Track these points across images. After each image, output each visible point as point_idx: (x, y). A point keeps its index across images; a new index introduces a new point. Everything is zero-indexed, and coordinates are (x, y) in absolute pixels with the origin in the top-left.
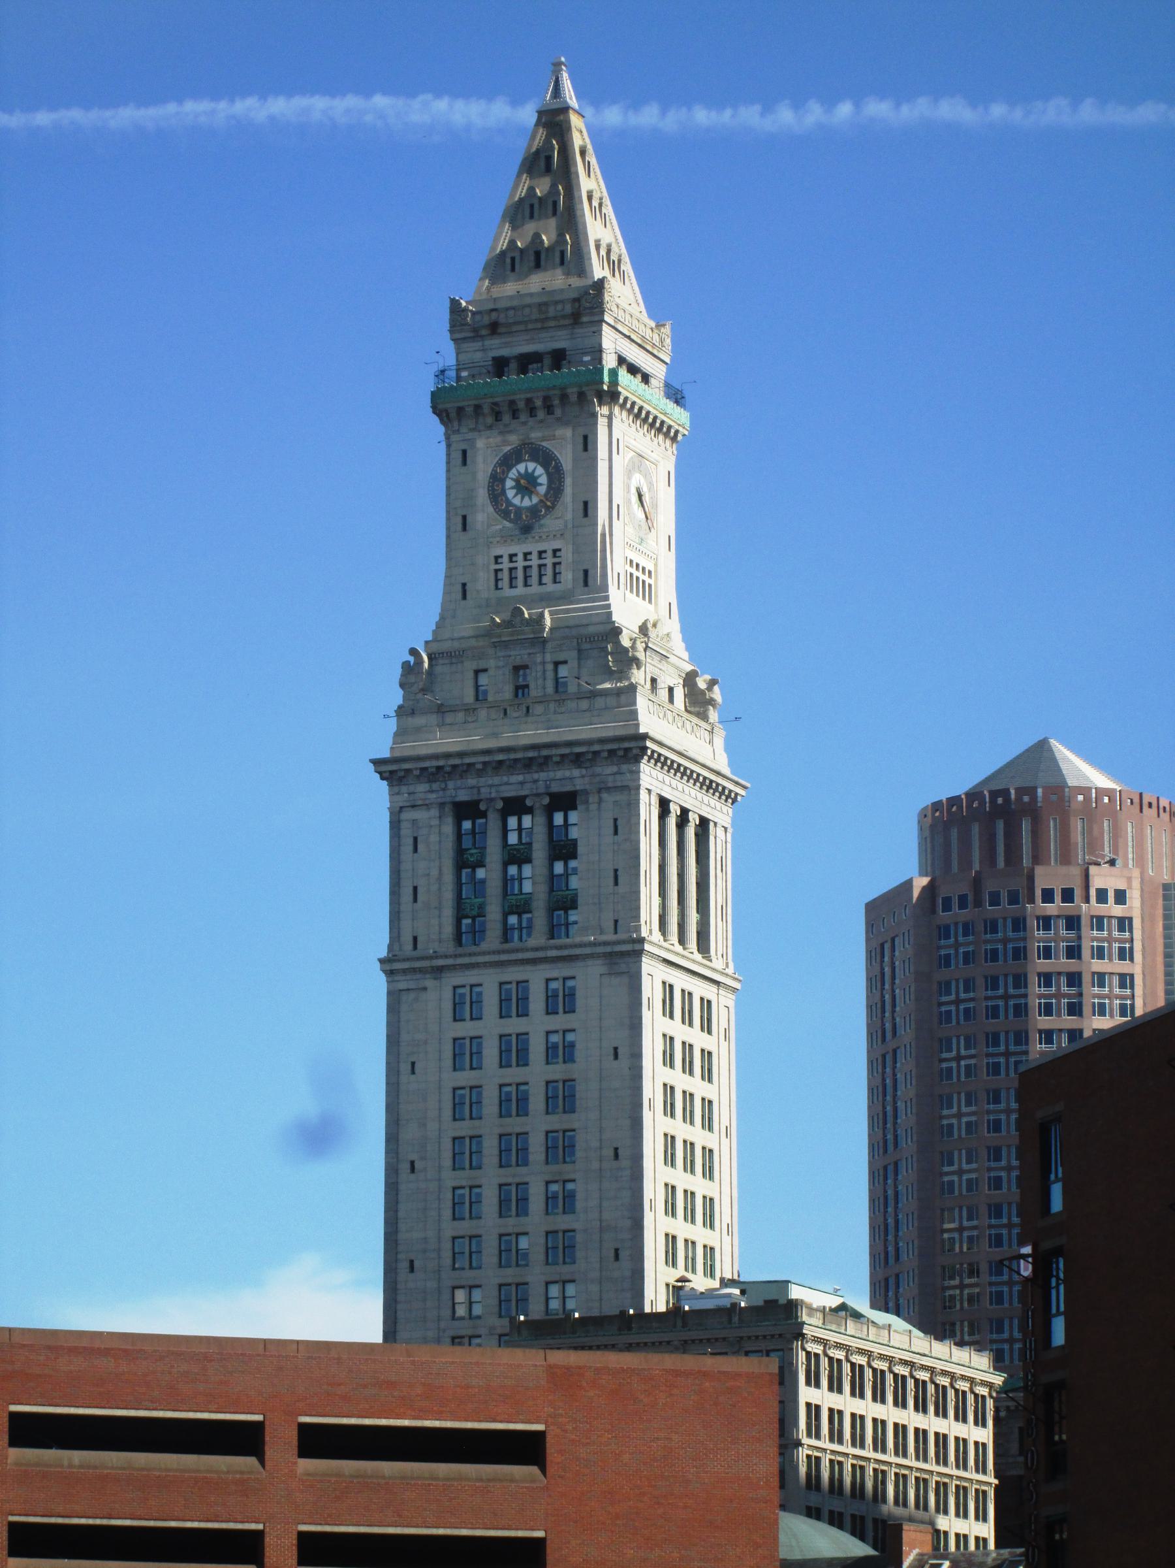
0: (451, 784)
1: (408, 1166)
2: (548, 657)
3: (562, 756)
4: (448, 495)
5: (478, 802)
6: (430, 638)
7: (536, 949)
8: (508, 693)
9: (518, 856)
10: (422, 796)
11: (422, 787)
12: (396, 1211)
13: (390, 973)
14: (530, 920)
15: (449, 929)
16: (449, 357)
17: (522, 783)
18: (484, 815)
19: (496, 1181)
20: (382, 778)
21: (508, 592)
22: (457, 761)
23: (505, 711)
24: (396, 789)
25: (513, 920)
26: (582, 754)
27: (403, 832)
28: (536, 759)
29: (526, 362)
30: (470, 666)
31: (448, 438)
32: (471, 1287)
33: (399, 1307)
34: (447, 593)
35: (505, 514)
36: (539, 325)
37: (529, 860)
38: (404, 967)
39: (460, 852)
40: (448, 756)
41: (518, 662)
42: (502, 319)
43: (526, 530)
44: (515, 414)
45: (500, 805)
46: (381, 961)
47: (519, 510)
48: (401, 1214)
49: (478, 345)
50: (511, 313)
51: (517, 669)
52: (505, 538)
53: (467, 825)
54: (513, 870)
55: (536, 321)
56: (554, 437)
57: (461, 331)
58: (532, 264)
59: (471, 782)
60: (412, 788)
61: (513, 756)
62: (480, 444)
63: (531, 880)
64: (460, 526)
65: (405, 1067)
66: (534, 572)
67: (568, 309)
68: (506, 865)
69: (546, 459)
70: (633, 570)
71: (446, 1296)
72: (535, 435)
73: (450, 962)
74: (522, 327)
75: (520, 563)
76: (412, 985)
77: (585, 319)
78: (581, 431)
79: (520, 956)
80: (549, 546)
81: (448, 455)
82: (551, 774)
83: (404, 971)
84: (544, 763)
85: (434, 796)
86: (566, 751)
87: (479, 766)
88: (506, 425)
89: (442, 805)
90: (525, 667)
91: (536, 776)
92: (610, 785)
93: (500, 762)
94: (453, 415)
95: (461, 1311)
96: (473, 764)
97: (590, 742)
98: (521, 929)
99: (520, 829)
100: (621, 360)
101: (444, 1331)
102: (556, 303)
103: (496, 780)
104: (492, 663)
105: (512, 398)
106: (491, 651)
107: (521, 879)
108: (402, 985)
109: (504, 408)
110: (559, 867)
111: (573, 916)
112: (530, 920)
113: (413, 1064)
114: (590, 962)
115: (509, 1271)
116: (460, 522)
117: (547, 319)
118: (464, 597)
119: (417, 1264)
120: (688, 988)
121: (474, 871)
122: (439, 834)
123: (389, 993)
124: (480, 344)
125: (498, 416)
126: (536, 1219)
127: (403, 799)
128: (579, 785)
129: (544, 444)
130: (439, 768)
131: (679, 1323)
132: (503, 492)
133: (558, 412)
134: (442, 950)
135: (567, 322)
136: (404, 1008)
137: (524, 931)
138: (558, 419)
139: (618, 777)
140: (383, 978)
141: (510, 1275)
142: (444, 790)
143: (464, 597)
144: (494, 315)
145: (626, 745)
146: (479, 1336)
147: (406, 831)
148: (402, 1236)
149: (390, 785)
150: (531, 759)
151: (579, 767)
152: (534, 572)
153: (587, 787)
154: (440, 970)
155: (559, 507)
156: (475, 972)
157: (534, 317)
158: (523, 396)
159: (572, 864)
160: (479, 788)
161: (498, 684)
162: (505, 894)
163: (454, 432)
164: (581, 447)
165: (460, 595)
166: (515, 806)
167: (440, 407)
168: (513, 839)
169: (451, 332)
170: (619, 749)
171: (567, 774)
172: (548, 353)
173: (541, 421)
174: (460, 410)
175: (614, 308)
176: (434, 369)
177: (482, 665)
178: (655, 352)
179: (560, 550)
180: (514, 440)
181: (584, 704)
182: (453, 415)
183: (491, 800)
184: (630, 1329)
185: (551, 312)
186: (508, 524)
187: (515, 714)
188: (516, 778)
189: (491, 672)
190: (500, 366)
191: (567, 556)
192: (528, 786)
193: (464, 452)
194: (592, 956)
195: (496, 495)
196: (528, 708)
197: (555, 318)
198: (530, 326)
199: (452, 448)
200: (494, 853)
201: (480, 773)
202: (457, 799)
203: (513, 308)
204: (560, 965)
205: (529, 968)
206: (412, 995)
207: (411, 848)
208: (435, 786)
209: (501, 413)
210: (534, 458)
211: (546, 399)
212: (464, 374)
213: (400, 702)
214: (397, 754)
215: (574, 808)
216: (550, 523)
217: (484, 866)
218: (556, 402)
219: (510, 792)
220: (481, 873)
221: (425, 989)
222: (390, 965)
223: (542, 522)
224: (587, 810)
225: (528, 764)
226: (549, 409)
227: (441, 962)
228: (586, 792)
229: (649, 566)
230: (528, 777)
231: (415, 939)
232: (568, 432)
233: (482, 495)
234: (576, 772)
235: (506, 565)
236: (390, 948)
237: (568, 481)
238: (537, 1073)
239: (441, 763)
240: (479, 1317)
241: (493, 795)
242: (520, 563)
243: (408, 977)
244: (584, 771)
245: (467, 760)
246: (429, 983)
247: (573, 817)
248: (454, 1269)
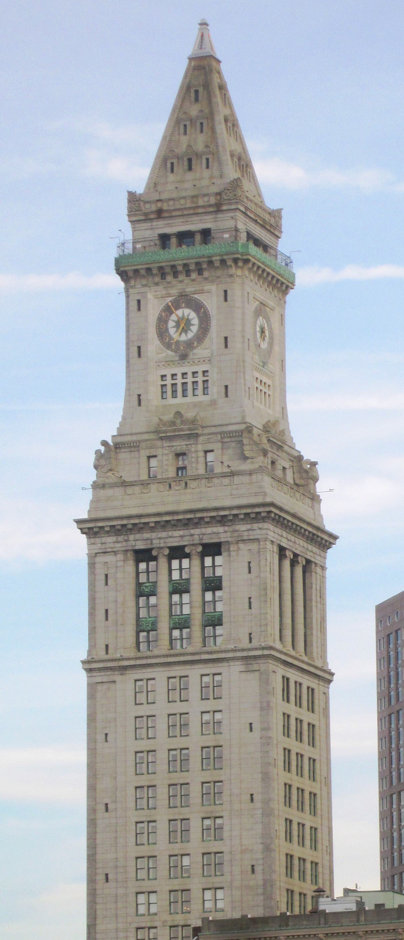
0: (132, 537)
1: (104, 807)
2: (200, 447)
3: (212, 517)
4: (128, 331)
5: (151, 550)
6: (115, 434)
7: (194, 654)
8: (171, 473)
9: (180, 588)
10: (112, 545)
11: (110, 540)
12: (95, 839)
13: (89, 671)
14: (190, 634)
15: (131, 640)
16: (127, 232)
17: (182, 537)
18: (155, 559)
19: (166, 818)
20: (83, 533)
21: (171, 401)
22: (136, 521)
23: (170, 485)
24: (92, 540)
25: (176, 633)
26: (225, 516)
27: (98, 571)
28: (192, 520)
29: (185, 237)
30: (144, 453)
31: (127, 290)
32: (149, 893)
33: (98, 907)
34: (127, 401)
35: (168, 346)
36: (191, 212)
37: (187, 591)
38: (100, 668)
39: (139, 585)
40: (130, 517)
41: (179, 450)
42: (165, 207)
43: (184, 357)
44: (176, 274)
45: (167, 552)
46: (83, 662)
48: (98, 842)
49: (148, 225)
50: (171, 203)
51: (178, 455)
52: (168, 363)
53: (143, 566)
54: (176, 598)
55: (190, 208)
56: (202, 292)
57: (135, 215)
58: (186, 167)
59: (146, 535)
60: (104, 540)
61: (176, 518)
62: (150, 296)
63: (190, 604)
64: (136, 354)
65: (100, 737)
66: (190, 387)
67: (213, 200)
68: (171, 594)
69: (198, 307)
70: (258, 385)
71: (132, 898)
73: (132, 663)
74: (179, 213)
75: (179, 381)
76: (105, 679)
77: (225, 208)
78: (223, 287)
79: (182, 659)
80: (200, 369)
81: (128, 303)
82: (204, 530)
83: (99, 669)
84: (198, 523)
85: (119, 545)
86: (213, 514)
87: (152, 525)
88: (169, 283)
90: (184, 454)
91: (192, 532)
92: (245, 538)
93: (167, 522)
95: (142, 910)
96: (148, 523)
97: (231, 508)
98: (182, 639)
99: (181, 569)
100: (250, 236)
101: (130, 924)
102: (205, 195)
103: (164, 534)
104: (159, 452)
106: (159, 443)
107: (181, 604)
108: (99, 679)
109: (168, 270)
110: (209, 596)
111: (219, 630)
112: (190, 634)
113: (106, 735)
114: (231, 663)
115: (176, 881)
116: (136, 351)
117: (198, 207)
118: (140, 404)
119: (110, 877)
120: (300, 680)
121: (148, 599)
122: (125, 572)
123: (89, 685)
124: (149, 224)
125: (163, 276)
126: (196, 844)
127: (97, 548)
128: (223, 538)
129: (196, 296)
130: (123, 526)
131: (322, 921)
132: (167, 330)
133: (206, 274)
134: (126, 655)
135: (212, 209)
136: (99, 695)
137: (184, 641)
138: (206, 279)
139: (251, 532)
141: (176, 884)
142: (126, 541)
143: (140, 404)
144: (159, 205)
145: (257, 510)
146: (155, 928)
147: (100, 571)
148: (99, 857)
149: (89, 538)
150: (189, 519)
151: (224, 525)
152: (190, 387)
153: (229, 539)
155: (207, 341)
156: (149, 670)
157: (188, 206)
158: (180, 262)
159: (218, 593)
160: (151, 540)
161: (165, 465)
162: (171, 615)
163: (132, 287)
164: (222, 298)
165: (136, 402)
166: (177, 553)
167: (122, 269)
168: (176, 576)
169: (129, 216)
170: (252, 513)
171: (215, 530)
172: (198, 232)
173: (194, 280)
174: (136, 271)
175: (245, 200)
176: (117, 242)
177: (153, 452)
178: (272, 230)
179: (207, 371)
180: (174, 291)
181: (226, 481)
182: (131, 274)
183: (161, 548)
184: (287, 925)
185: (201, 202)
186: (170, 353)
187: (177, 488)
188: (177, 533)
189: (160, 458)
190: (164, 240)
191: (213, 377)
192: (187, 538)
193: (139, 301)
194: (233, 659)
195: (162, 333)
196: (186, 483)
197: (203, 207)
198: (186, 212)
199: (131, 298)
200: (164, 588)
201: (152, 529)
202: (137, 548)
203: (173, 199)
204: (210, 665)
205: (188, 667)
206: (105, 686)
207: (103, 582)
208: (121, 538)
209: (164, 273)
210: (188, 306)
211: (198, 264)
212: (139, 246)
213: (94, 478)
214: (93, 516)
216: (200, 352)
217: (155, 595)
218: (205, 266)
219: (175, 543)
220: (153, 600)
221: (114, 682)
222: (90, 666)
223: (195, 351)
224: (229, 555)
225: (187, 524)
226: (200, 271)
227: (126, 663)
228: (228, 542)
229: (269, 382)
230: (186, 532)
231: (107, 646)
232: (213, 288)
234: (221, 529)
235: (169, 381)
236: (89, 651)
237: (214, 323)
238: (195, 740)
239: (125, 522)
240: (155, 914)
241: (162, 545)
242: (179, 381)
243: (103, 674)
244: (226, 528)
246: (118, 678)
247: (219, 560)
248: (137, 880)
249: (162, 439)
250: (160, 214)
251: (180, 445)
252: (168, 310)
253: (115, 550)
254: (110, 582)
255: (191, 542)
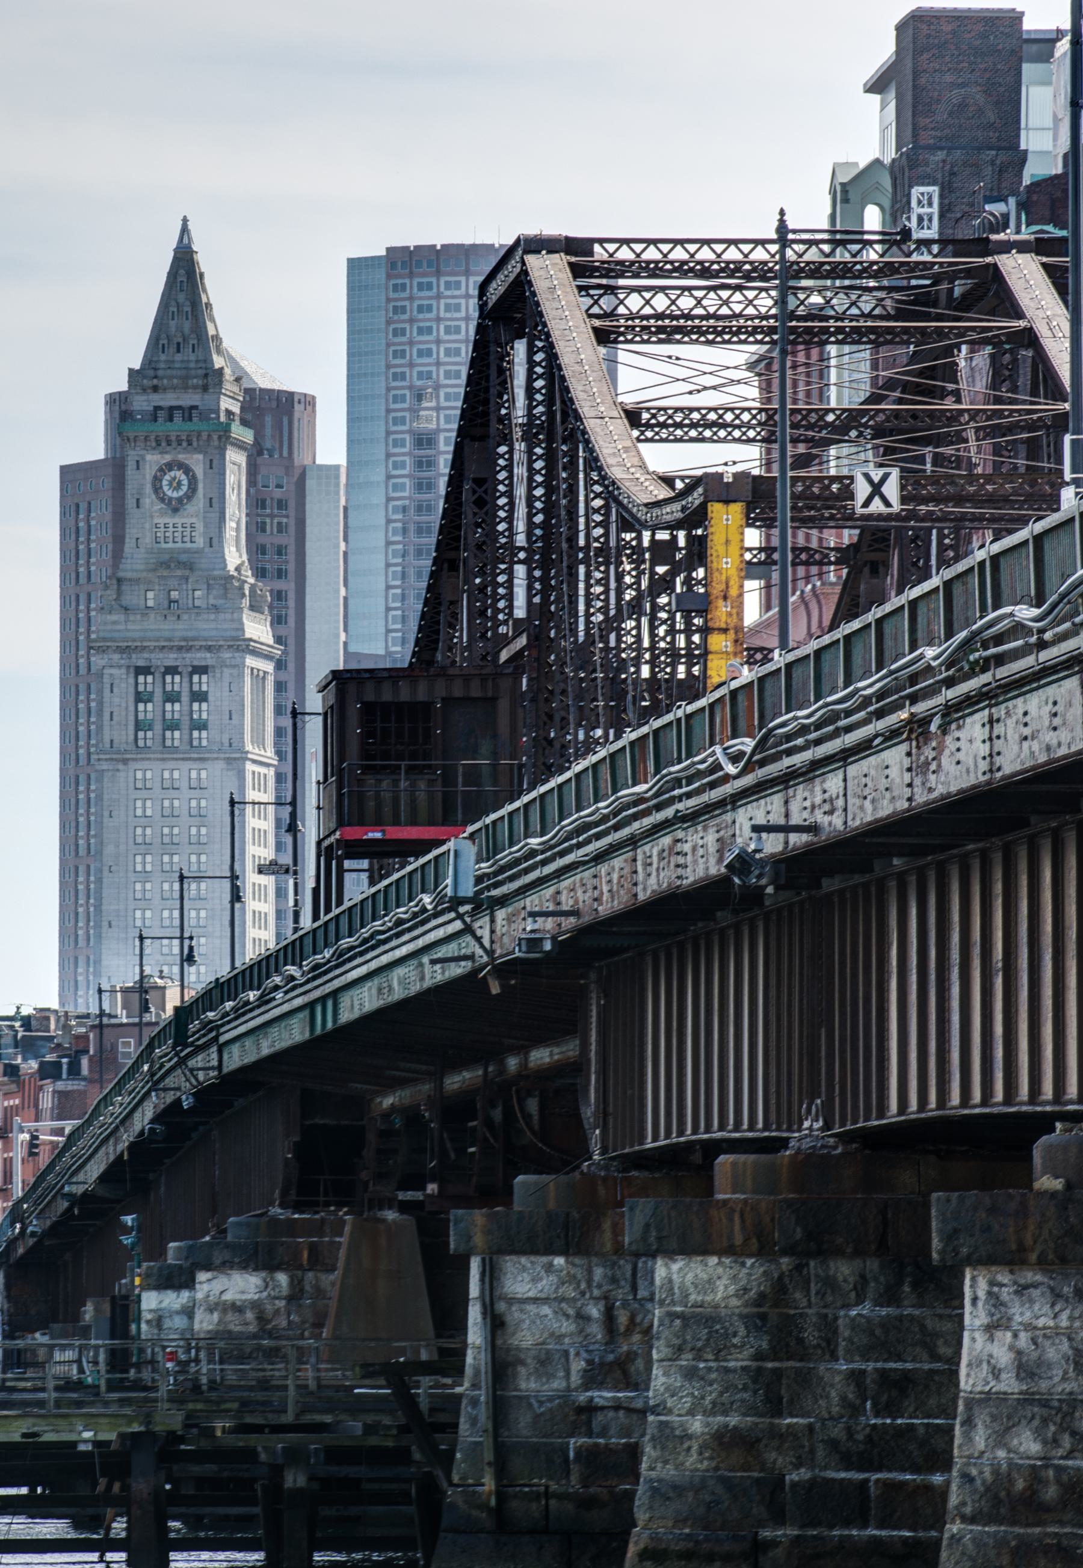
11: (116, 657)
35: (162, 500)
37: (179, 701)
39: (138, 694)
43: (176, 510)
47: (171, 499)
52: (162, 514)
59: (146, 655)
69: (187, 470)
72: (181, 457)
80: (188, 521)
89: (128, 667)
103: (161, 655)
128: (210, 662)
155: (195, 501)
166: (172, 670)
180: (168, 458)
188: (172, 656)
195: (157, 489)
216: (190, 508)
225: (180, 648)
232: (201, 457)
233: (148, 489)
234: (208, 655)
237: (200, 486)
246: (121, 767)
247: (204, 678)
254: (115, 690)
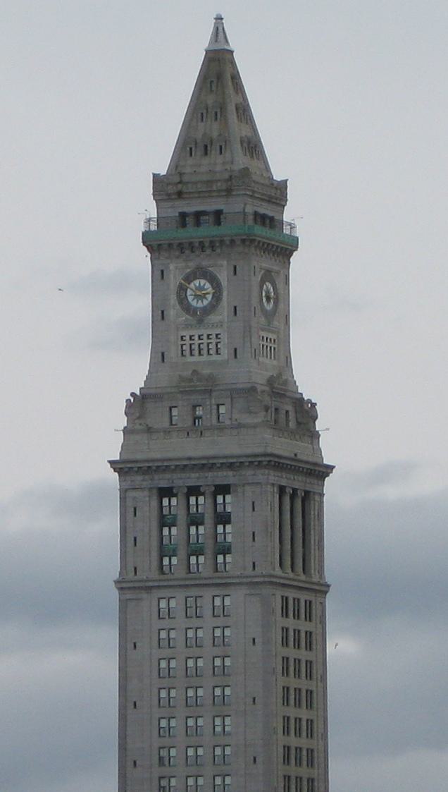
0: (156, 477)
6: (143, 385)
9: (196, 521)
11: (139, 478)
13: (121, 589)
21: (190, 359)
22: (160, 464)
26: (234, 463)
28: (206, 465)
30: (167, 404)
37: (202, 524)
42: (185, 190)
49: (170, 204)
52: (187, 326)
59: (168, 476)
60: (133, 478)
62: (172, 267)
64: (160, 317)
69: (213, 280)
77: (234, 193)
80: (213, 332)
83: (129, 588)
84: (212, 467)
85: (145, 483)
86: (225, 461)
92: (250, 482)
93: (185, 466)
94: (155, 248)
103: (183, 475)
105: (192, 240)
106: (179, 396)
108: (128, 596)
120: (297, 596)
129: (210, 269)
133: (218, 250)
140: (116, 592)
142: (151, 480)
145: (260, 459)
147: (130, 503)
154: (151, 588)
156: (171, 590)
158: (197, 240)
164: (232, 273)
166: (194, 491)
169: (154, 195)
176: (143, 218)
178: (278, 202)
179: (220, 334)
180: (192, 265)
181: (235, 432)
191: (224, 338)
193: (162, 272)
195: (182, 300)
201: (174, 471)
202: (160, 486)
208: (147, 477)
209: (183, 248)
211: (211, 242)
214: (125, 457)
215: (229, 493)
216: (213, 318)
227: (151, 584)
228: (235, 484)
233: (173, 299)
234: (231, 473)
237: (225, 293)
244: (235, 473)
245: (166, 464)
246: (144, 595)
247: (228, 498)
249: (182, 392)
250: (180, 194)
251: (195, 398)
252: (189, 279)
253: (142, 487)
255: (206, 483)
